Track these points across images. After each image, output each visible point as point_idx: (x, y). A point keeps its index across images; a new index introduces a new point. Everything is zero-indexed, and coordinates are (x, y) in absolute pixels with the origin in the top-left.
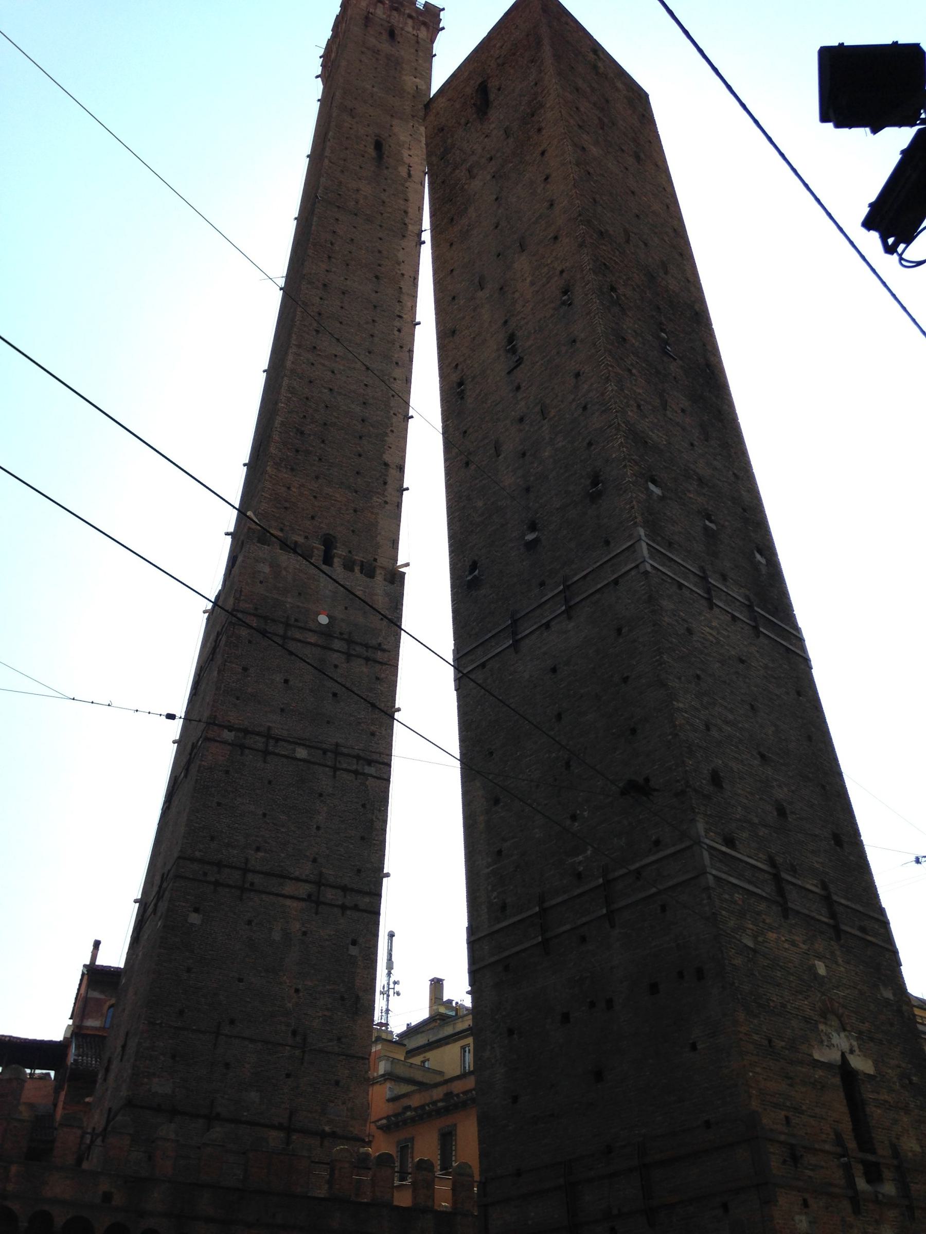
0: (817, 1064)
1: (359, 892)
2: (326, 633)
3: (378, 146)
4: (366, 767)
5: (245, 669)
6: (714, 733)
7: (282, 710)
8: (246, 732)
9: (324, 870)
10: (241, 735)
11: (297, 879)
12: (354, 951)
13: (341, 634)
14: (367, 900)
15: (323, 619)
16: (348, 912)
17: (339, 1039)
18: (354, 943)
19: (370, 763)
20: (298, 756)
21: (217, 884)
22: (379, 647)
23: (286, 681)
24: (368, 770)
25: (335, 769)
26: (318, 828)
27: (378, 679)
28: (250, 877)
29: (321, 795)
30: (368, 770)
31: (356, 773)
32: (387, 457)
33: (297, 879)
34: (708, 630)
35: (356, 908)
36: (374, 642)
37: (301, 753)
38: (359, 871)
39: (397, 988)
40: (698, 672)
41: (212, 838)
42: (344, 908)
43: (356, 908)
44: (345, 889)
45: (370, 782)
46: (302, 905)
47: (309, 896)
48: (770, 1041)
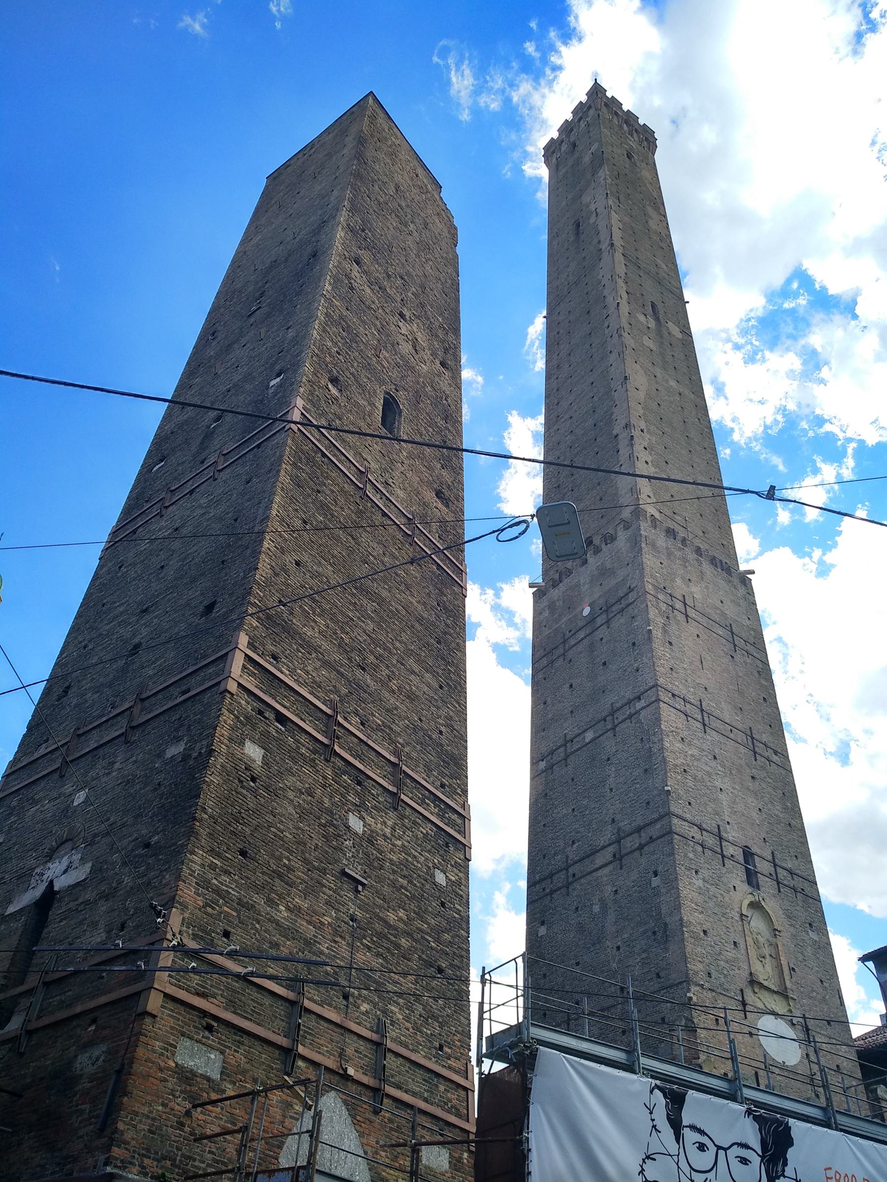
1: (648, 825)
2: (592, 619)
3: (578, 225)
4: (637, 704)
5: (545, 703)
7: (572, 712)
8: (552, 753)
9: (621, 824)
10: (549, 758)
11: (604, 847)
12: (656, 881)
14: (658, 826)
15: (587, 611)
16: (646, 848)
17: (658, 976)
18: (656, 874)
19: (639, 698)
20: (587, 740)
21: (552, 892)
22: (631, 590)
23: (571, 686)
24: (639, 705)
25: (614, 728)
26: (611, 790)
27: (633, 617)
28: (571, 871)
29: (609, 759)
31: (630, 717)
32: (615, 433)
33: (604, 847)
35: (652, 840)
36: (625, 590)
37: (589, 736)
38: (648, 803)
41: (544, 856)
42: (641, 847)
43: (652, 840)
44: (639, 830)
46: (610, 867)
47: (614, 856)
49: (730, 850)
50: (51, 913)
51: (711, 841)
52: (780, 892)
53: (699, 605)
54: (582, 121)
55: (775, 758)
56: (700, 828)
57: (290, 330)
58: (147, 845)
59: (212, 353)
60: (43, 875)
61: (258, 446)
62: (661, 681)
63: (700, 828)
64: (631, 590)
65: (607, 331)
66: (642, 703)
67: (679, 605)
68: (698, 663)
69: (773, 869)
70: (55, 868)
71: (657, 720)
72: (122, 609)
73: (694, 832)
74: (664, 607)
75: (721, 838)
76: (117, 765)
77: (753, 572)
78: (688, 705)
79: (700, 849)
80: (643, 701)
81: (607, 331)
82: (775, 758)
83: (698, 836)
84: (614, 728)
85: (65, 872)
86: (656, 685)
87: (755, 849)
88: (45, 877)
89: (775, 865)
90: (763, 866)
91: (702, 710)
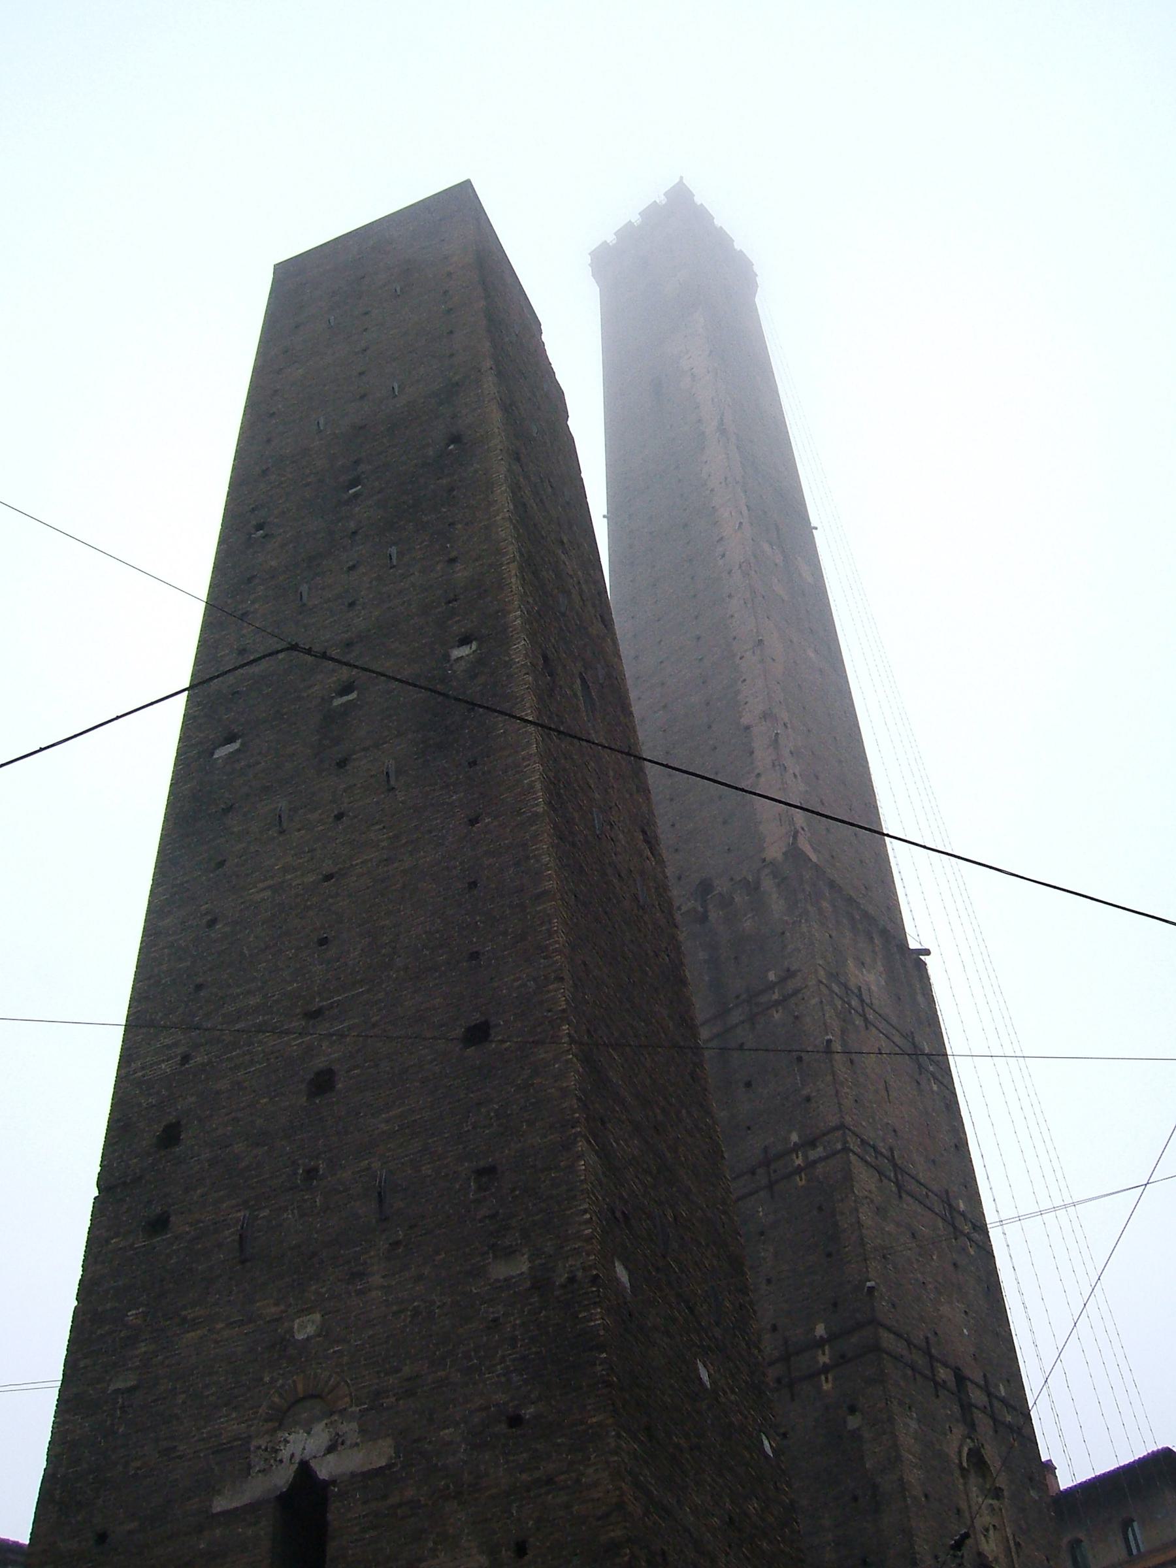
6: (199, 1059)
12: (853, 1422)
13: (737, 997)
14: (854, 1340)
18: (852, 1410)
19: (813, 1144)
24: (813, 1155)
25: (770, 1186)
26: (769, 1281)
27: (797, 1017)
30: (813, 1155)
32: (744, 721)
34: (261, 885)
38: (835, 1305)
40: (199, 980)
45: (820, 1169)
49: (943, 1373)
50: (330, 1517)
51: (921, 1361)
52: (996, 1432)
53: (875, 1002)
55: (976, 1236)
56: (909, 1343)
57: (458, 566)
58: (515, 1421)
59: (273, 563)
60: (276, 1451)
62: (848, 1120)
63: (909, 1343)
64: (790, 974)
65: (721, 562)
66: (819, 1152)
67: (855, 1002)
68: (884, 1093)
69: (986, 1399)
70: (304, 1443)
71: (848, 1177)
72: (253, 1001)
73: (900, 1348)
74: (839, 1003)
75: (931, 1357)
76: (377, 1280)
77: (927, 952)
78: (880, 1158)
79: (910, 1372)
80: (820, 1149)
81: (721, 562)
82: (976, 1236)
83: (905, 1353)
84: (770, 1186)
85: (331, 1449)
86: (842, 1126)
87: (967, 1372)
88: (285, 1454)
89: (989, 1395)
90: (977, 1396)
91: (895, 1165)
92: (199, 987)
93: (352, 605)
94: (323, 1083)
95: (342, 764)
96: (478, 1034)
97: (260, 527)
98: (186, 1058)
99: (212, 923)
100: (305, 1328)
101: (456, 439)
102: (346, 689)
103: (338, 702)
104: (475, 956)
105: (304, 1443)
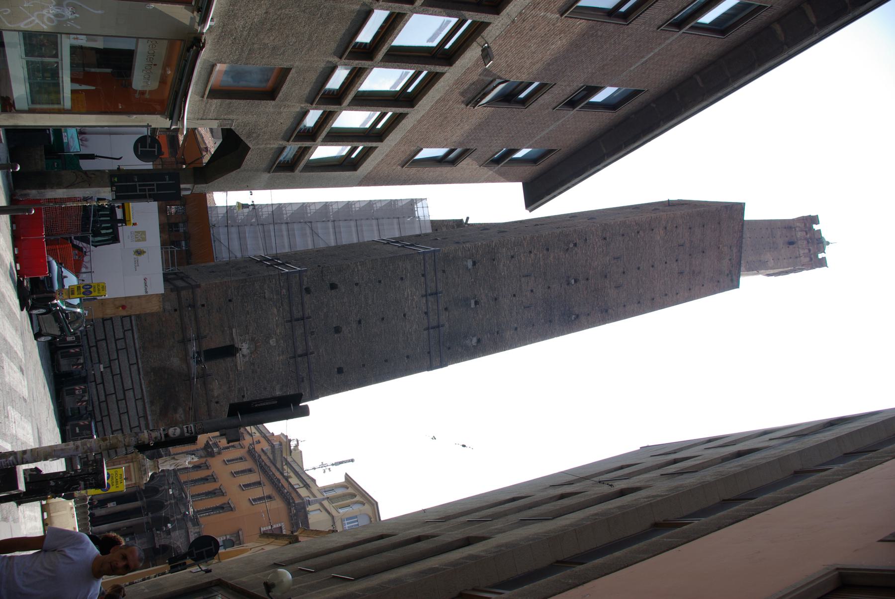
0: (231, 328)
6: (356, 289)
39: (327, 471)
48: (230, 301)
54: (806, 251)
61: (429, 353)
72: (370, 302)
92: (380, 282)
93: (514, 295)
94: (338, 330)
95: (446, 309)
96: (340, 371)
97: (575, 245)
98: (357, 284)
99: (402, 279)
100: (272, 342)
101: (577, 316)
102: (476, 303)
103: (473, 302)
104: (364, 365)
105: (245, 348)
